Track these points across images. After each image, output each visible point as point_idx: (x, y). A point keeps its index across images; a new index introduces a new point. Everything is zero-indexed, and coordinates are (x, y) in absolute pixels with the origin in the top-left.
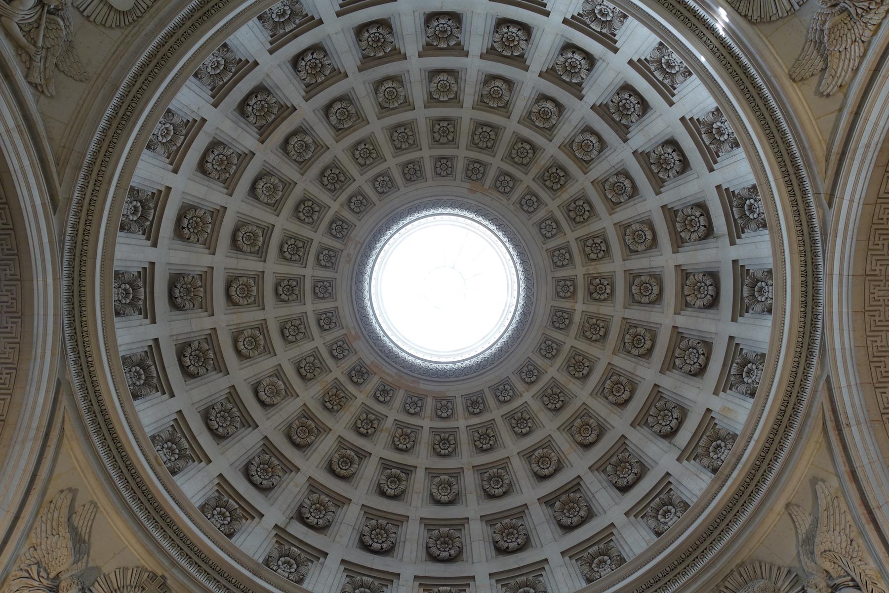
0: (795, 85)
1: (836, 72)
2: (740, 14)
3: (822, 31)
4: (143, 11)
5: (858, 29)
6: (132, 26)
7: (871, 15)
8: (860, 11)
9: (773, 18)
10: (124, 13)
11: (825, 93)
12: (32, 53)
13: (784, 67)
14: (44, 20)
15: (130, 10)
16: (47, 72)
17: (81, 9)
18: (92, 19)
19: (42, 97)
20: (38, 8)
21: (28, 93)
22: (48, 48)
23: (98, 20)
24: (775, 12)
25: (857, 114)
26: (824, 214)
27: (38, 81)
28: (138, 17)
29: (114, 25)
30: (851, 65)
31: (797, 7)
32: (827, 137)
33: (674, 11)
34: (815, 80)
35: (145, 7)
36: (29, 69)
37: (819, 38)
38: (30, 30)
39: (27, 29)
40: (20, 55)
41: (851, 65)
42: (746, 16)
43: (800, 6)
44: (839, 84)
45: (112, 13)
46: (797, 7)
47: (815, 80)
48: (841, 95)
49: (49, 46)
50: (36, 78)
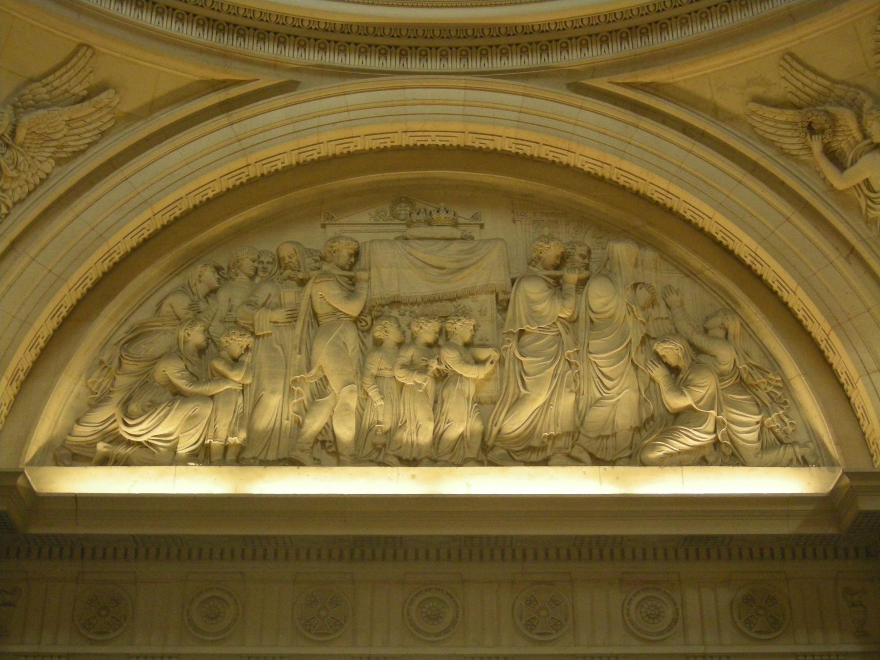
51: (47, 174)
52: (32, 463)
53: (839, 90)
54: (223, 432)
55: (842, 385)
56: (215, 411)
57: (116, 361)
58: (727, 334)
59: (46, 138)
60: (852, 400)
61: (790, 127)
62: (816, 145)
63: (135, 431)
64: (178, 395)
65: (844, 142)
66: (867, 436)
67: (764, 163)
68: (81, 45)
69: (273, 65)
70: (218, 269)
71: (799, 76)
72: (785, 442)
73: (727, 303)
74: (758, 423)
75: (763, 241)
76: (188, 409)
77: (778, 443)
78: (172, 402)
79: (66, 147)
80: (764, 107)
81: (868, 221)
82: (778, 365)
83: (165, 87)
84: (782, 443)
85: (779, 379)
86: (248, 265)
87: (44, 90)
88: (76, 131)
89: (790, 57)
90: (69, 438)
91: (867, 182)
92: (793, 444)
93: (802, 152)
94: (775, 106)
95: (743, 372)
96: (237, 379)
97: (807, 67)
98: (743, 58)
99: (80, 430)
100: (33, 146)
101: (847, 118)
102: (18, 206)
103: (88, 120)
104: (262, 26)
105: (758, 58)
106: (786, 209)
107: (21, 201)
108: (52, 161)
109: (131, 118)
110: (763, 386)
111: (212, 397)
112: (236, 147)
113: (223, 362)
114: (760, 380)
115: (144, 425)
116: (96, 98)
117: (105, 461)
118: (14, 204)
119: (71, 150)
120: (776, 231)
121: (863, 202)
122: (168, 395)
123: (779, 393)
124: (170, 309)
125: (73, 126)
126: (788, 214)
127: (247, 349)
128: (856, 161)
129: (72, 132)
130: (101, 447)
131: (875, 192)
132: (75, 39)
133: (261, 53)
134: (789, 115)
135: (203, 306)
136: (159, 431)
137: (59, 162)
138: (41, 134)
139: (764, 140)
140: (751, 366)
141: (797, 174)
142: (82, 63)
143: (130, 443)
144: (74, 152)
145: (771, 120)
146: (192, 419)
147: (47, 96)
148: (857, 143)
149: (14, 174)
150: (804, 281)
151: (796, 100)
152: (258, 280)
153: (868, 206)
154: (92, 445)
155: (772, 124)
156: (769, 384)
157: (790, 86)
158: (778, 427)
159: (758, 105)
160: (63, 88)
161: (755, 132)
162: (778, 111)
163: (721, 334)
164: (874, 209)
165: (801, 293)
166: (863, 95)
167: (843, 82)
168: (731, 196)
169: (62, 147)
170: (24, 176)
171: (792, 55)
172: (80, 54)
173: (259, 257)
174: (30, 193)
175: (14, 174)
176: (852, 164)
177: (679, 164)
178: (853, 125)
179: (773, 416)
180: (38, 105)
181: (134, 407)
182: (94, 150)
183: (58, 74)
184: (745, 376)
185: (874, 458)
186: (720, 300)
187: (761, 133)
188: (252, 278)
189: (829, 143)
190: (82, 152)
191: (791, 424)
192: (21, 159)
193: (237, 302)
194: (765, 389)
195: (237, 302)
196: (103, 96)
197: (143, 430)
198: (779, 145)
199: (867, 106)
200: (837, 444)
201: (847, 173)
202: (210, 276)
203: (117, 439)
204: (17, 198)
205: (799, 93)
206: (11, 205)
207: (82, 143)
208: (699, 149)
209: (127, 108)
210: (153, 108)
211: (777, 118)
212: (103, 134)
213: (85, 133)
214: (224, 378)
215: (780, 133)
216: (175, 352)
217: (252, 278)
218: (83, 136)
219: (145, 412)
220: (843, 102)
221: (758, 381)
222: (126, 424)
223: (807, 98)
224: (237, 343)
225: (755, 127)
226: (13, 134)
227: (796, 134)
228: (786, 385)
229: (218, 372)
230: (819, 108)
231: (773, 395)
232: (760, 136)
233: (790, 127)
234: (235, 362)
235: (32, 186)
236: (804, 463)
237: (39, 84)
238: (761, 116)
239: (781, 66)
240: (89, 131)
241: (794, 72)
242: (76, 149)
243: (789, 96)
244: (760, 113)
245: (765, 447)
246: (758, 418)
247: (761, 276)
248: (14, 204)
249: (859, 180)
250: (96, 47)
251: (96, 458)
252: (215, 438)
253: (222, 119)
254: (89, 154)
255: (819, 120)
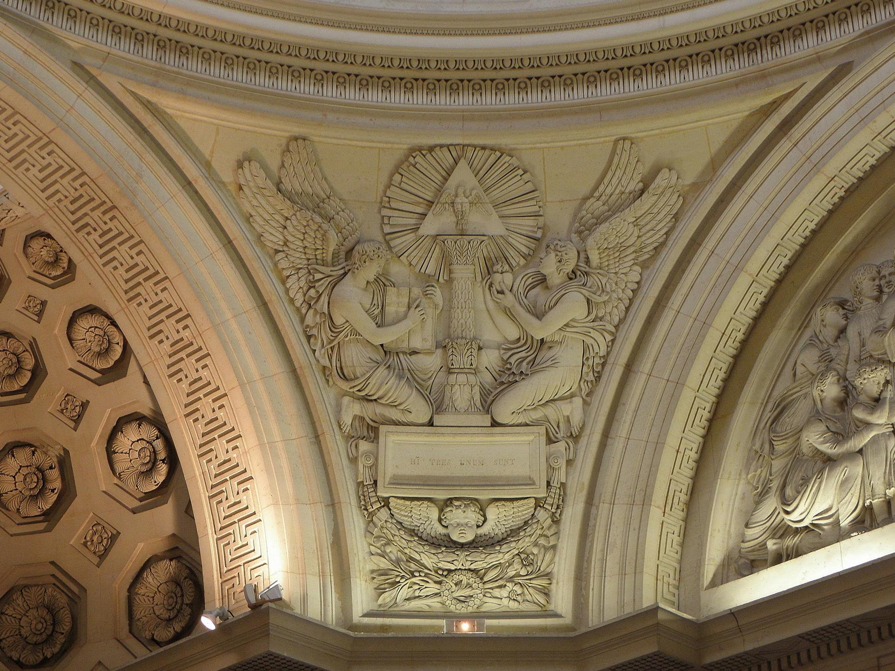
0: (287, 134)
1: (264, 195)
2: (441, 146)
3: (330, 219)
5: (298, 258)
7: (302, 283)
8: (318, 276)
9: (397, 177)
11: (246, 164)
13: (321, 139)
24: (403, 185)
25: (188, 185)
26: (69, 47)
30: (258, 219)
31: (386, 212)
32: (183, 124)
33: (526, 63)
34: (274, 163)
37: (324, 208)
41: (258, 219)
42: (431, 149)
43: (383, 217)
44: (245, 189)
46: (386, 212)
47: (274, 163)
48: (227, 177)
51: (637, 283)
52: (713, 584)
54: (880, 488)
56: (866, 466)
57: (767, 446)
59: (621, 248)
63: (795, 516)
64: (830, 461)
68: (616, 142)
69: (819, 59)
70: (842, 304)
76: (839, 474)
78: (821, 471)
79: (645, 247)
83: (719, 139)
86: (868, 287)
87: (600, 203)
88: (648, 227)
90: (743, 545)
96: (882, 421)
99: (751, 533)
100: (611, 262)
102: (621, 326)
103: (655, 211)
104: (795, 21)
107: (621, 321)
108: (638, 268)
109: (698, 186)
111: (860, 451)
112: (808, 166)
113: (862, 407)
115: (802, 507)
116: (653, 186)
117: (778, 559)
118: (617, 327)
119: (651, 248)
122: (819, 464)
124: (803, 369)
125: (642, 223)
127: (887, 382)
129: (644, 230)
130: (771, 545)
132: (608, 139)
133: (799, 54)
135: (833, 352)
136: (819, 508)
137: (644, 265)
138: (614, 248)
142: (624, 159)
143: (797, 531)
144: (655, 248)
146: (845, 484)
147: (606, 207)
149: (605, 298)
152: (885, 297)
154: (764, 545)
160: (617, 191)
169: (642, 248)
170: (615, 295)
172: (618, 151)
173: (879, 272)
174: (627, 309)
175: (605, 298)
180: (600, 220)
181: (789, 491)
182: (673, 237)
183: (606, 181)
188: (878, 299)
190: (663, 244)
192: (604, 281)
193: (866, 333)
195: (866, 333)
196: (657, 181)
197: (806, 510)
202: (831, 316)
203: (782, 531)
204: (616, 320)
206: (613, 330)
207: (659, 237)
209: (689, 178)
210: (714, 165)
212: (676, 217)
213: (657, 224)
214: (868, 425)
216: (816, 415)
217: (878, 299)
218: (657, 229)
219: (799, 492)
222: (787, 513)
224: (871, 381)
226: (587, 261)
229: (861, 421)
234: (877, 402)
235: (627, 302)
237: (592, 200)
240: (660, 221)
242: (655, 245)
248: (617, 327)
250: (633, 135)
251: (770, 559)
252: (873, 496)
253: (785, 145)
254: (670, 243)
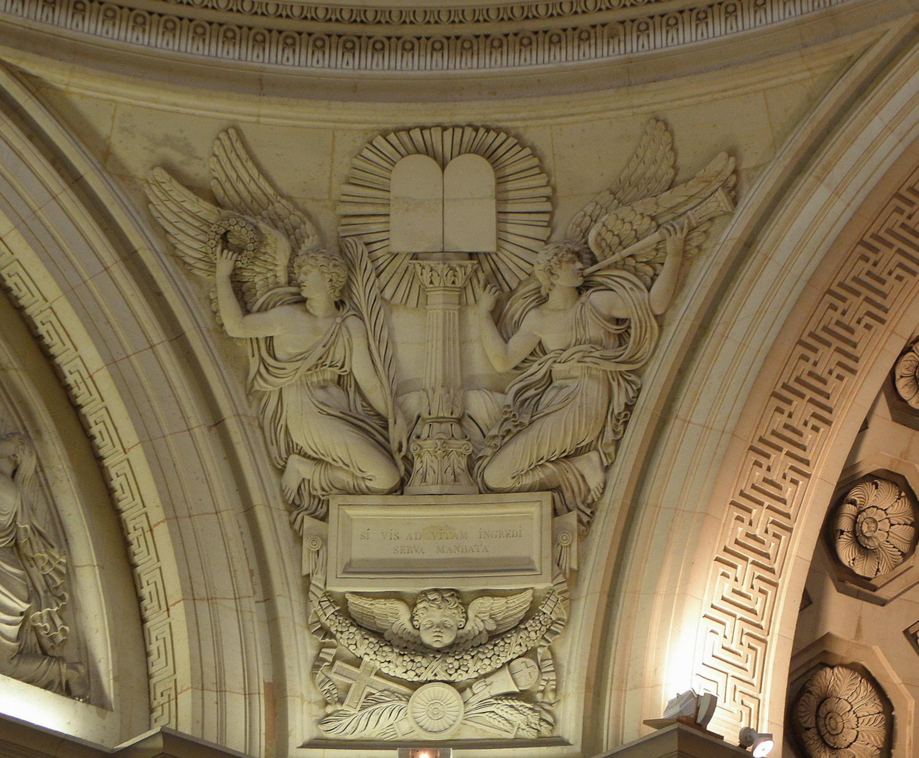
4: (458, 132)
6: (500, 124)
10: (490, 155)
12: (680, 236)
14: (611, 259)
15: (476, 152)
16: (694, 191)
17: (546, 217)
18: (548, 191)
19: (744, 166)
20: (599, 279)
21: (754, 197)
22: (653, 218)
23: (541, 180)
27: (720, 195)
28: (476, 130)
29: (527, 151)
35: (448, 134)
36: (711, 220)
38: (644, 272)
39: (649, 270)
40: (699, 247)
45: (508, 171)
49: (647, 220)
50: (721, 199)
53: (281, 206)
55: (140, 599)
58: (15, 472)
60: (148, 625)
61: (197, 224)
62: (224, 265)
65: (261, 277)
66: (153, 681)
67: (147, 257)
71: (238, 164)
72: (50, 653)
73: (24, 428)
74: (22, 614)
75: (112, 363)
77: (40, 652)
80: (174, 182)
81: (250, 392)
82: (66, 540)
84: (45, 653)
85: (64, 561)
89: (234, 132)
91: (270, 340)
92: (60, 659)
93: (200, 265)
94: (190, 188)
95: (22, 533)
97: (252, 158)
98: (175, 105)
101: (278, 250)
105: (193, 115)
106: (155, 333)
110: (41, 564)
114: (40, 554)
120: (133, 358)
121: (254, 364)
123: (59, 582)
126: (156, 340)
128: (266, 310)
131: (275, 358)
134: (204, 208)
139: (154, 223)
140: (34, 529)
141: (183, 290)
145: (178, 204)
148: (277, 285)
150: (148, 441)
151: (219, 192)
153: (259, 372)
155: (175, 209)
156: (49, 563)
157: (220, 170)
158: (45, 628)
159: (167, 176)
161: (149, 210)
162: (192, 196)
163: (8, 469)
164: (265, 381)
165: (138, 456)
166: (308, 228)
167: (289, 198)
168: (90, 283)
171: (239, 132)
176: (259, 311)
177: (35, 208)
178: (282, 260)
179: (44, 611)
184: (23, 540)
185: (155, 715)
186: (16, 418)
187: (155, 214)
189: (241, 268)
191: (63, 630)
194: (43, 569)
198: (174, 241)
199: (308, 244)
200: (116, 679)
201: (249, 318)
205: (228, 186)
208: (68, 199)
211: (187, 205)
215: (182, 226)
220: (280, 224)
221: (38, 554)
223: (236, 197)
225: (151, 202)
227: (201, 237)
228: (69, 574)
230: (248, 218)
231: (50, 581)
232: (152, 216)
233: (197, 224)
236: (66, 690)
238: (165, 193)
239: (218, 139)
241: (233, 156)
243: (213, 183)
244: (166, 187)
245: (22, 653)
246: (25, 606)
247: (80, 406)
249: (262, 334)
255: (241, 233)
